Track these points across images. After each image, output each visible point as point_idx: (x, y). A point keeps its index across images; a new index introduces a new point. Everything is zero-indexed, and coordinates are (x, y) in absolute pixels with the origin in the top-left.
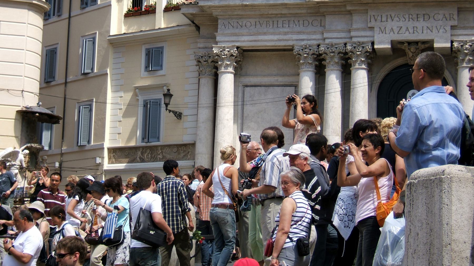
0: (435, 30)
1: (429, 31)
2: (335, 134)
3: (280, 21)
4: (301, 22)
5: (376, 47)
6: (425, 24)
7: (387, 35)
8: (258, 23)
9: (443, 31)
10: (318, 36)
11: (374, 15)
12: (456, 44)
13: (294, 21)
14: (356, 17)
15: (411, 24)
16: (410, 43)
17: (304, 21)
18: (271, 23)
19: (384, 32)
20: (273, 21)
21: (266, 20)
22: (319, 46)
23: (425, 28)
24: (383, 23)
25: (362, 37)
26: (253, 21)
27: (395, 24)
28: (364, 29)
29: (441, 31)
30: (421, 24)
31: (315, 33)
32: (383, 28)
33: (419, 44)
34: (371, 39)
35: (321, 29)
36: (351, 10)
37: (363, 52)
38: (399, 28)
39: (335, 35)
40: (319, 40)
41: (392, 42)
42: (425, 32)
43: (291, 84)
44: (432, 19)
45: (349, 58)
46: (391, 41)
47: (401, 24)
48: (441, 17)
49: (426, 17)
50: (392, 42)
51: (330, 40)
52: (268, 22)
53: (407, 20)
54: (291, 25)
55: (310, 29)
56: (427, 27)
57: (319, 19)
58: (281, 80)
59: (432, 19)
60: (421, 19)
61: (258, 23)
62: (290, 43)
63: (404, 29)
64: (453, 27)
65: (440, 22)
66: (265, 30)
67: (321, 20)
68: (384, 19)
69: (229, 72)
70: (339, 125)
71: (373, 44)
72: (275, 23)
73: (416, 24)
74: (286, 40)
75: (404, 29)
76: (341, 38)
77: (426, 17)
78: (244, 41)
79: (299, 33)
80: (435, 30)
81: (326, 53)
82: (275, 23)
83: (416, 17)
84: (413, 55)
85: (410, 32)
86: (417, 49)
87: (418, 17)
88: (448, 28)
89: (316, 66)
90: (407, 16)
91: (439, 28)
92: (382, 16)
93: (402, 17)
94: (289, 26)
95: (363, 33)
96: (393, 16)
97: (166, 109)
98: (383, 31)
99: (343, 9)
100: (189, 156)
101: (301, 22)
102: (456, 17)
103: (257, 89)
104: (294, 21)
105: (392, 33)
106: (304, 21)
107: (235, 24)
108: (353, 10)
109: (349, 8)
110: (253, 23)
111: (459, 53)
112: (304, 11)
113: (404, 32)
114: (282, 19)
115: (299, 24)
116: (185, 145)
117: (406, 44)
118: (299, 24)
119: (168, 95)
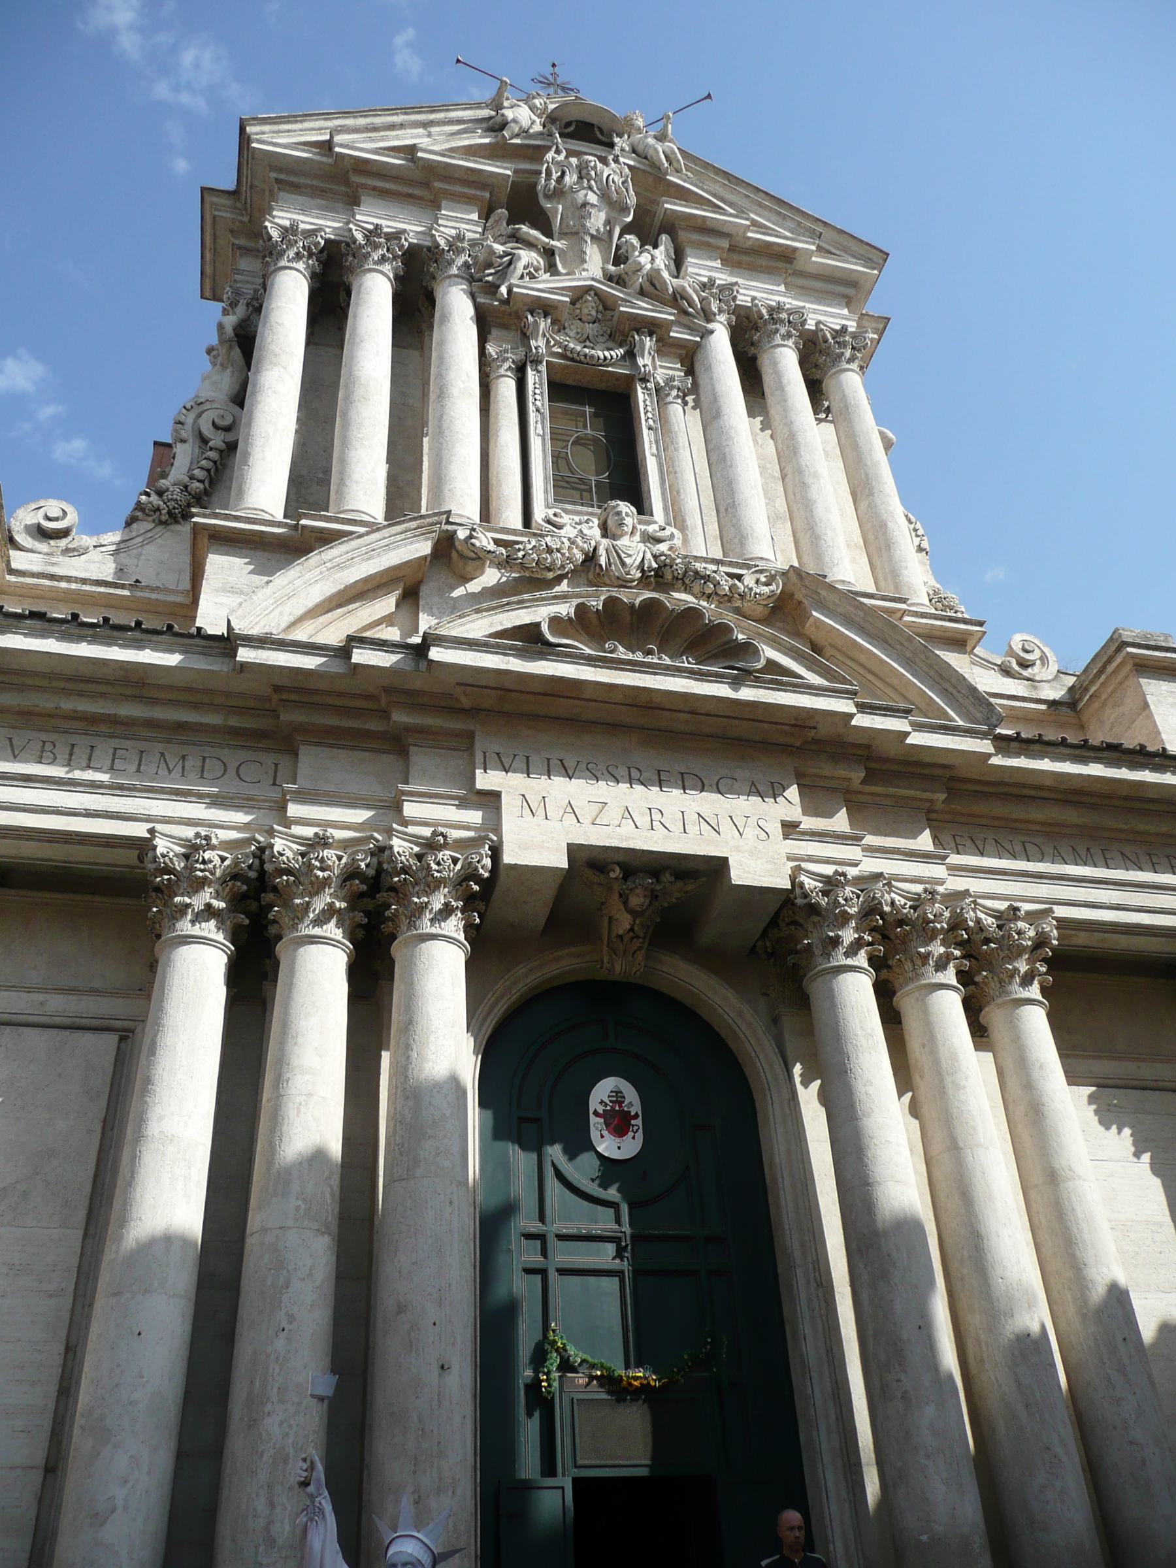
1: (704, 826)
2: (315, 1226)
5: (508, 858)
7: (553, 824)
9: (756, 833)
11: (498, 754)
13: (162, 754)
17: (204, 758)
19: (541, 812)
20: (73, 745)
29: (751, 832)
33: (667, 877)
36: (408, 729)
38: (595, 808)
43: (106, 1023)
46: (570, 846)
50: (573, 850)
52: (48, 746)
57: (269, 759)
58: (58, 1005)
67: (276, 765)
70: (332, 1182)
75: (613, 813)
83: (657, 777)
84: (632, 930)
85: (638, 826)
86: (654, 896)
87: (662, 778)
92: (528, 758)
93: (605, 773)
94: (138, 771)
99: (375, 725)
104: (162, 754)
106: (208, 761)
108: (420, 731)
109: (400, 717)
113: (617, 823)
114: (115, 743)
115: (183, 768)
117: (616, 873)
118: (183, 768)
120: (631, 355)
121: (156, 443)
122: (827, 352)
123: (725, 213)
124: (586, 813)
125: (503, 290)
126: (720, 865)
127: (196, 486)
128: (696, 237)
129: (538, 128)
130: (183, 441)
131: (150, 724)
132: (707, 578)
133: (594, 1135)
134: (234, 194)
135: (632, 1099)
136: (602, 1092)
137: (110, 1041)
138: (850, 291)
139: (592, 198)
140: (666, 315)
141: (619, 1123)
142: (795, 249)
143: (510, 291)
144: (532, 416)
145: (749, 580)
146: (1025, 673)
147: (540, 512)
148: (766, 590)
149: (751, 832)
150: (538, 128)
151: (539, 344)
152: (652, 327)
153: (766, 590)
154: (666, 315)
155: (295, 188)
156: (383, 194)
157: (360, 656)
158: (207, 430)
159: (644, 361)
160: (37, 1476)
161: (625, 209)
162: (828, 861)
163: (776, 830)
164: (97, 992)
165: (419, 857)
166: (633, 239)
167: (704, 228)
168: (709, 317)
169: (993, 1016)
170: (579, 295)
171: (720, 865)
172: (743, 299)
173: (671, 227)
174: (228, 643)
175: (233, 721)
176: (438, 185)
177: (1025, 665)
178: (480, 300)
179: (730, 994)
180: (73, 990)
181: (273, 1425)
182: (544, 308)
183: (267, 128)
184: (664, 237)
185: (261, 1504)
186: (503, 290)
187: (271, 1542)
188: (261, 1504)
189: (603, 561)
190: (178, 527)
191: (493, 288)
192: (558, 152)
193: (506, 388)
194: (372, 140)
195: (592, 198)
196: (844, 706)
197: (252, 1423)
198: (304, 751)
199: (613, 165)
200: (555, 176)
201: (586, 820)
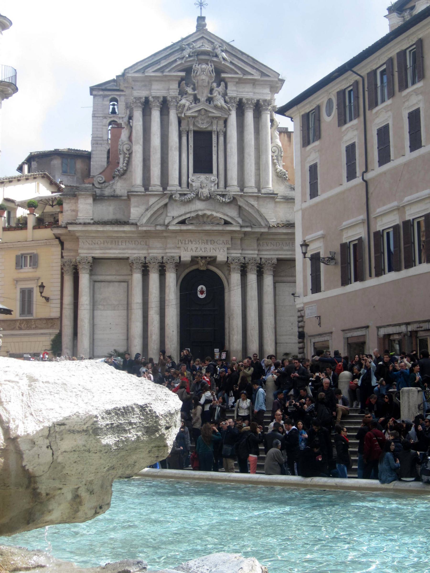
0: (217, 250)
1: (214, 251)
3: (120, 240)
4: (133, 242)
5: (182, 259)
6: (212, 246)
8: (105, 242)
10: (145, 252)
12: (230, 258)
15: (203, 246)
16: (202, 257)
18: (114, 243)
21: (111, 240)
22: (145, 258)
23: (212, 249)
24: (186, 245)
25: (173, 253)
26: (102, 240)
27: (193, 246)
28: (174, 248)
29: (221, 250)
30: (209, 246)
31: (143, 249)
32: (186, 248)
33: (208, 258)
34: (178, 254)
35: (146, 247)
37: (174, 263)
39: (155, 251)
40: (145, 254)
42: (212, 251)
44: (216, 244)
45: (165, 266)
47: (197, 246)
48: (221, 242)
49: (212, 242)
51: (152, 254)
53: (201, 243)
54: (127, 244)
56: (213, 248)
58: (118, 278)
59: (216, 244)
60: (209, 243)
61: (105, 242)
62: (127, 255)
63: (199, 249)
64: (228, 249)
65: (221, 245)
66: (110, 246)
68: (187, 242)
71: (180, 257)
72: (117, 242)
73: (206, 246)
74: (124, 253)
75: (199, 249)
76: (160, 253)
77: (212, 242)
78: (96, 253)
79: (133, 249)
80: (217, 250)
81: (149, 263)
82: (117, 242)
86: (206, 261)
88: (226, 249)
89: (143, 271)
90: (200, 241)
91: (220, 248)
95: (173, 251)
96: (192, 240)
97: (41, 296)
98: (186, 250)
100: (55, 327)
101: (133, 242)
102: (230, 242)
103: (102, 283)
105: (192, 251)
107: (90, 242)
109: (165, 234)
110: (102, 242)
111: (231, 264)
112: (135, 235)
114: (121, 240)
116: (52, 319)
117: (199, 258)
119: (42, 286)
124: (194, 250)
127: (125, 168)
135: (204, 288)
137: (126, 284)
143: (185, 114)
149: (221, 250)
156: (157, 81)
166: (215, 85)
173: (223, 80)
180: (120, 275)
185: (153, 345)
187: (154, 349)
188: (153, 345)
189: (199, 196)
190: (123, 177)
191: (181, 113)
194: (153, 68)
197: (151, 337)
200: (195, 72)
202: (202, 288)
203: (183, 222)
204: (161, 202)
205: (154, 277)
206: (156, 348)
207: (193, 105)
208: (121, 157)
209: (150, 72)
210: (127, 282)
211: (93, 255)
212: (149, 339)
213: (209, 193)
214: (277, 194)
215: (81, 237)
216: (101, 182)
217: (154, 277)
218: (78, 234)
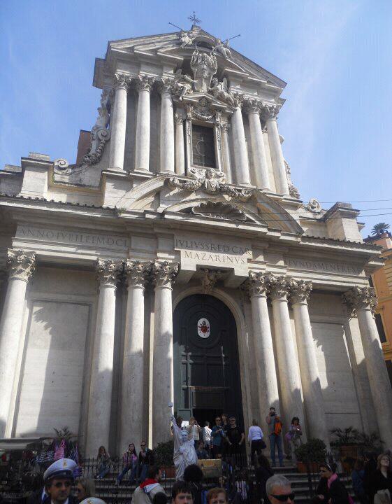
4: (106, 240)
5: (182, 268)
14: (161, 241)
29: (240, 262)
31: (119, 251)
36: (157, 233)
41: (197, 265)
50: (197, 265)
55: (114, 247)
69: (22, 280)
72: (79, 237)
82: (79, 237)
99: (150, 232)
108: (160, 233)
109: (156, 230)
120: (214, 117)
121: (81, 131)
122: (267, 114)
123: (243, 72)
124: (201, 258)
125: (181, 98)
126: (232, 270)
128: (233, 78)
129: (191, 43)
130: (94, 140)
131: (96, 230)
132: (233, 192)
133: (199, 332)
134: (104, 60)
136: (200, 322)
138: (275, 94)
139: (205, 67)
140: (225, 106)
141: (204, 329)
142: (261, 82)
144: (188, 137)
145: (243, 192)
146: (313, 210)
147: (190, 168)
148: (247, 195)
149: (240, 262)
150: (191, 43)
151: (190, 114)
152: (220, 109)
153: (247, 195)
154: (225, 106)
155: (123, 62)
156: (147, 64)
157: (148, 216)
158: (100, 137)
159: (218, 120)
160: (79, 404)
161: (214, 70)
162: (258, 269)
163: (246, 261)
164: (83, 295)
165: (161, 267)
167: (236, 75)
168: (236, 106)
169: (295, 307)
170: (201, 99)
171: (232, 270)
172: (246, 97)
173: (226, 75)
174: (115, 211)
175: (116, 230)
176: (162, 62)
177: (313, 208)
178: (174, 100)
179: (231, 298)
181: (133, 397)
182: (192, 104)
183: (116, 44)
184: (225, 79)
185: (131, 414)
186: (181, 98)
188: (131, 414)
192: (196, 52)
193: (181, 127)
195: (205, 67)
196: (265, 230)
198: (132, 237)
199: (212, 56)
201: (201, 258)
202: (204, 323)
203: (188, 212)
204: (154, 184)
205: (138, 295)
206: (136, 417)
207: (192, 92)
208: (94, 144)
209: (141, 50)
210: (90, 306)
211: (38, 252)
212: (125, 400)
213: (220, 185)
214: (302, 202)
215: (18, 223)
216: (62, 166)
217: (138, 295)
218: (15, 218)
